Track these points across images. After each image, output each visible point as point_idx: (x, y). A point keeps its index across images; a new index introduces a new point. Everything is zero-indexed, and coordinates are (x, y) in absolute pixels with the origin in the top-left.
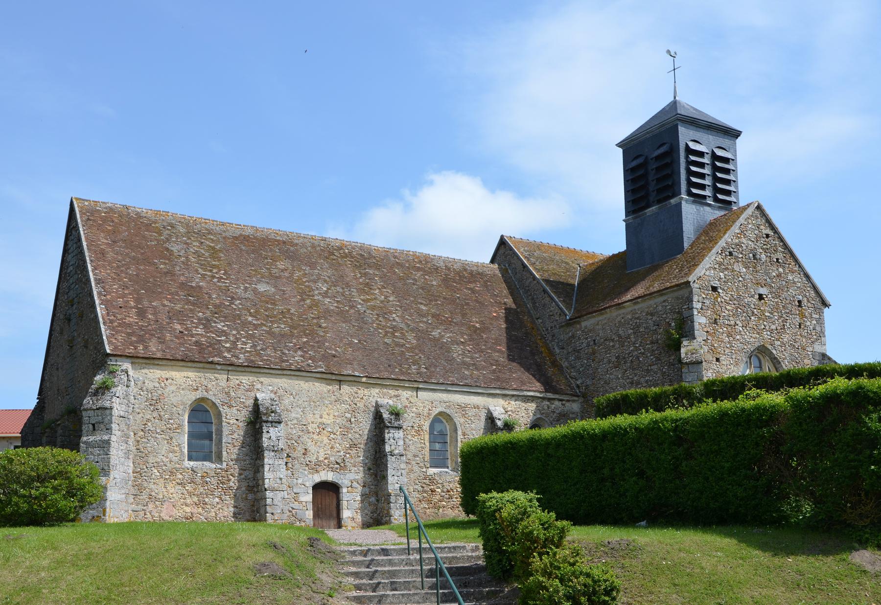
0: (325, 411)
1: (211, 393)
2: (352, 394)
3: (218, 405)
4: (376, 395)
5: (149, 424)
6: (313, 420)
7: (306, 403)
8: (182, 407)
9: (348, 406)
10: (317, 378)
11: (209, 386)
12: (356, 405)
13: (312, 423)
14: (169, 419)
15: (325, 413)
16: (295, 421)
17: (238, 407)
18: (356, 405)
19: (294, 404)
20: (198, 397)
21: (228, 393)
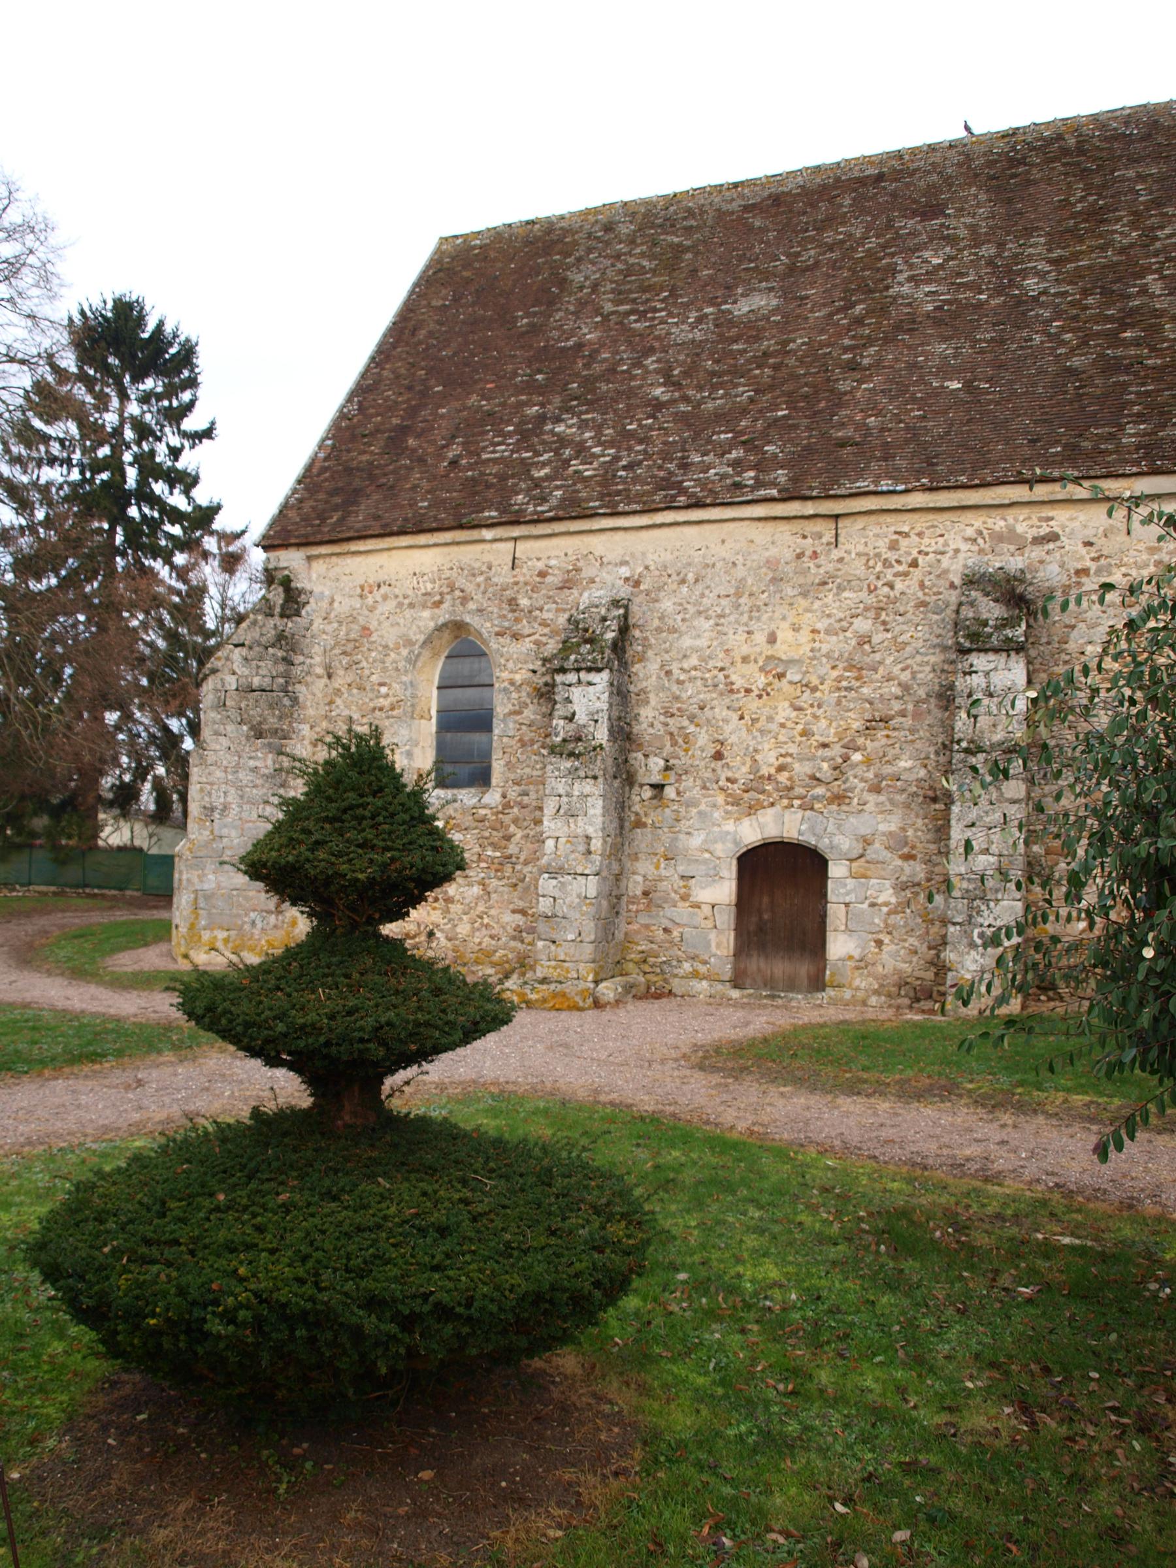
0: (784, 618)
1: (472, 606)
2: (878, 555)
3: (486, 635)
4: (964, 547)
5: (339, 701)
6: (745, 650)
7: (724, 602)
8: (405, 652)
9: (863, 594)
10: (759, 519)
11: (470, 588)
12: (892, 587)
13: (745, 659)
14: (381, 684)
15: (785, 625)
16: (694, 661)
17: (536, 637)
18: (892, 587)
19: (692, 609)
20: (441, 621)
21: (512, 602)
